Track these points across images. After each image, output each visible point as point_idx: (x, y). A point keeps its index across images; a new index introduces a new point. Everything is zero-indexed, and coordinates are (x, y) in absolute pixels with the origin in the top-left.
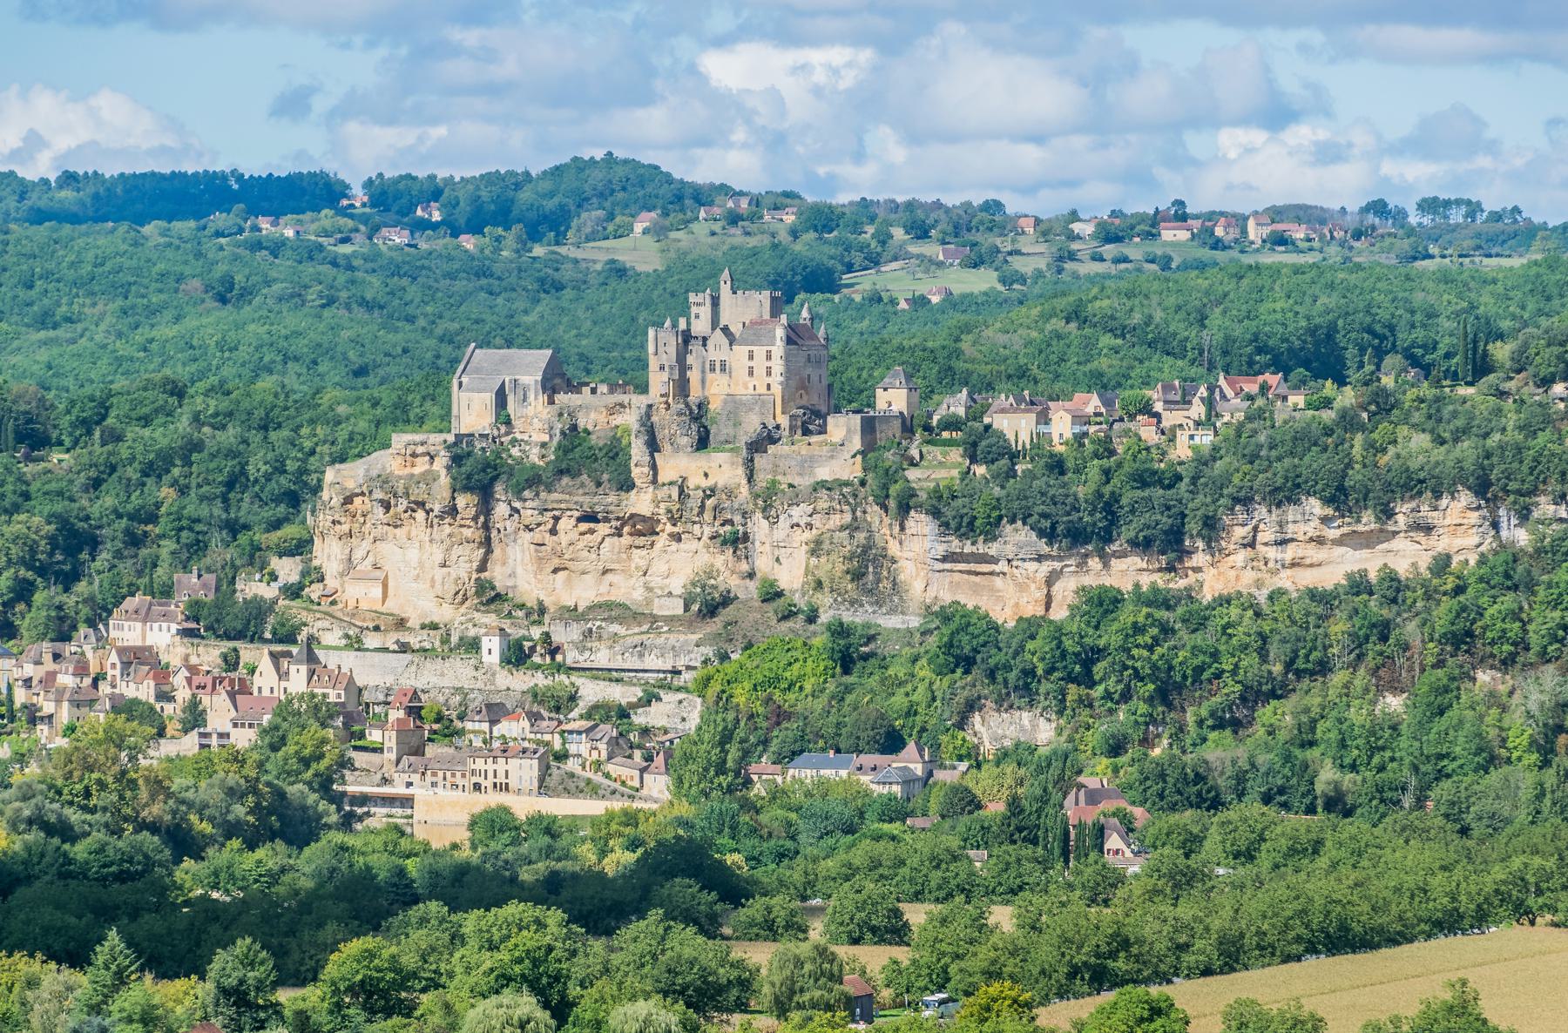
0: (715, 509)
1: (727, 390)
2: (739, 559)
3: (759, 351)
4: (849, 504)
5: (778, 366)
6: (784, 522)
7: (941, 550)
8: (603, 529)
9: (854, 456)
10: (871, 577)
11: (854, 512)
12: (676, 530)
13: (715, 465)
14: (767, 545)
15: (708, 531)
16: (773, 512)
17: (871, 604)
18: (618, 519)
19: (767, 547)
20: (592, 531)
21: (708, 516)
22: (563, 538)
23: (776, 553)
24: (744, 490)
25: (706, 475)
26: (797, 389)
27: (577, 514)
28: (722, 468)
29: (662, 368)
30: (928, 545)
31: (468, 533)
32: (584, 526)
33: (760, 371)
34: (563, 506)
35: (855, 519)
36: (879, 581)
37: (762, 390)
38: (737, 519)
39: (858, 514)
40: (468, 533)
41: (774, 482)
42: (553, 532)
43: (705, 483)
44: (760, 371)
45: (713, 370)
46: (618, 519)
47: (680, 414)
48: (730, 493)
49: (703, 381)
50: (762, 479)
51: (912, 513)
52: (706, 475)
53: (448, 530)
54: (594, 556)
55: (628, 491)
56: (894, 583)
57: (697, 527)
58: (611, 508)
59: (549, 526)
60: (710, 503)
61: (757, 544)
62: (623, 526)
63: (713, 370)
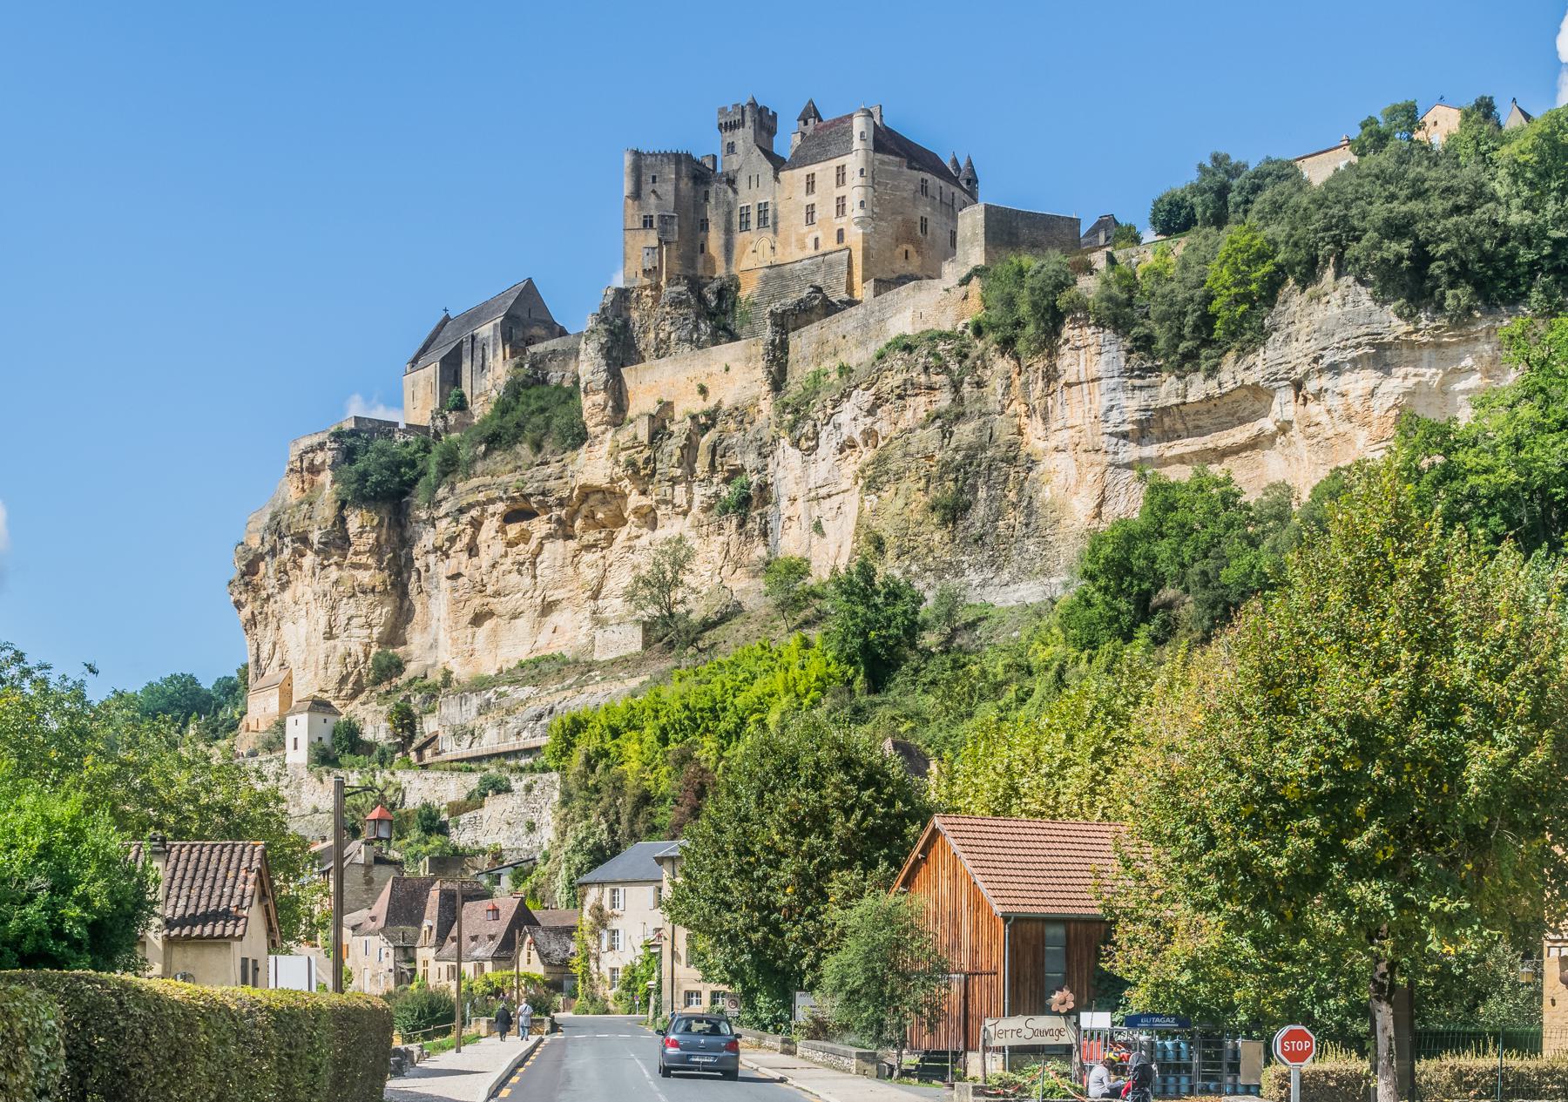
1: (768, 258)
2: (749, 537)
3: (824, 171)
4: (946, 369)
5: (854, 191)
6: (827, 447)
7: (1132, 406)
8: (540, 527)
9: (965, 281)
11: (956, 387)
13: (717, 368)
15: (700, 493)
16: (808, 428)
18: (561, 503)
20: (525, 537)
21: (701, 466)
22: (485, 559)
23: (816, 513)
24: (767, 407)
25: (703, 390)
26: (898, 241)
27: (501, 507)
28: (732, 374)
29: (647, 223)
30: (1102, 403)
31: (364, 577)
32: (513, 530)
33: (825, 210)
34: (481, 497)
35: (958, 399)
36: (999, 515)
37: (829, 244)
38: (751, 460)
39: (966, 389)
40: (364, 577)
41: (816, 376)
42: (472, 550)
43: (699, 405)
45: (745, 226)
46: (561, 503)
47: (677, 303)
48: (741, 414)
50: (799, 374)
51: (1067, 332)
52: (703, 390)
53: (334, 573)
54: (527, 580)
55: (575, 447)
56: (1030, 511)
57: (680, 490)
58: (551, 484)
59: (466, 539)
60: (706, 440)
61: (784, 503)
62: (572, 517)
63: (745, 226)
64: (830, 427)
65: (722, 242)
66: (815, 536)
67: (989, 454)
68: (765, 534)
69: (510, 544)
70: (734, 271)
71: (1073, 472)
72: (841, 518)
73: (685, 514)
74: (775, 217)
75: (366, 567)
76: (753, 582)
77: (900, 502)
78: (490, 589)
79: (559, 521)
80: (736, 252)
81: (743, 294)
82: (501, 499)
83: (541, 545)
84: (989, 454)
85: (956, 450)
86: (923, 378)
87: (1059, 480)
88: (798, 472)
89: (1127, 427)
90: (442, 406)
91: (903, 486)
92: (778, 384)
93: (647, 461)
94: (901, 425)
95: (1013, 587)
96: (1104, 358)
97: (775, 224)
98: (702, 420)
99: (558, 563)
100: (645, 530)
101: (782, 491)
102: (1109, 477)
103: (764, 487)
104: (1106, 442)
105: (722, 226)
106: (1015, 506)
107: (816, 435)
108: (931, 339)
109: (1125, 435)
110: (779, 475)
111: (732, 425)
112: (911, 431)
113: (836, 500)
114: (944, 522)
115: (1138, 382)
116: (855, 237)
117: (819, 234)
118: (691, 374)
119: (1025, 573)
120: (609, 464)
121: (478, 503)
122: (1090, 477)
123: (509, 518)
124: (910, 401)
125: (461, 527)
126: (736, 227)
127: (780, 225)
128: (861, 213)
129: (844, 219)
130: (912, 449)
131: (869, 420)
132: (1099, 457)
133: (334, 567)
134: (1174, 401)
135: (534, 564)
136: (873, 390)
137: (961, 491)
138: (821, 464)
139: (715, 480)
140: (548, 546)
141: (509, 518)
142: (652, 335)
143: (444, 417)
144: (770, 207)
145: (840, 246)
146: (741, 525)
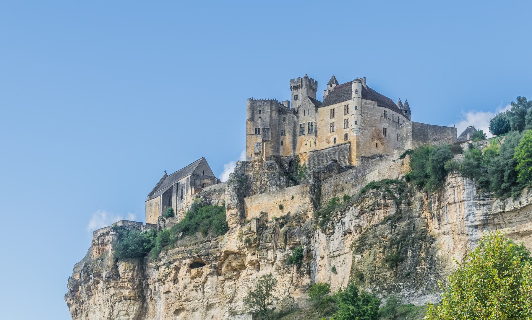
0: (286, 234)
1: (313, 147)
2: (302, 274)
3: (339, 107)
4: (394, 198)
5: (353, 117)
6: (338, 233)
7: (479, 213)
8: (206, 270)
9: (402, 157)
10: (409, 261)
11: (398, 204)
12: (255, 258)
13: (288, 197)
14: (326, 259)
15: (280, 255)
16: (329, 225)
17: (408, 288)
18: (216, 259)
19: (326, 259)
20: (199, 274)
22: (181, 284)
24: (311, 214)
25: (281, 207)
27: (188, 261)
28: (296, 201)
30: (465, 211)
32: (194, 271)
33: (339, 125)
34: (179, 256)
35: (399, 211)
36: (417, 263)
38: (303, 239)
39: (403, 206)
40: (126, 292)
41: (334, 200)
42: (175, 280)
43: (279, 214)
44: (339, 125)
46: (216, 259)
47: (270, 167)
48: (299, 218)
49: (294, 143)
50: (326, 199)
51: (449, 179)
52: (281, 207)
54: (200, 294)
55: (223, 234)
56: (432, 262)
58: (212, 250)
59: (172, 276)
61: (318, 259)
63: (302, 132)
64: (340, 224)
65: (291, 140)
66: (333, 274)
67: (413, 236)
68: (309, 273)
69: (193, 278)
70: (297, 153)
71: (452, 244)
72: (344, 265)
73: (273, 264)
74: (316, 128)
75: (127, 288)
76: (303, 295)
77: (371, 258)
78: (183, 298)
79: (215, 267)
80: (298, 145)
81: (301, 164)
82: (189, 257)
83: (206, 278)
84: (413, 236)
85: (398, 234)
86: (382, 201)
87: (445, 248)
88: (325, 245)
89: (477, 223)
90: (162, 215)
91: (373, 251)
92: (316, 204)
93: (255, 240)
94: (372, 223)
95: (423, 297)
96: (466, 191)
97: (316, 132)
98: (281, 221)
99: (215, 286)
100: (254, 271)
101: (318, 253)
102: (468, 246)
103: (309, 251)
104: (466, 230)
105: (292, 133)
106: (425, 259)
107: (334, 227)
108: (387, 183)
109: (476, 227)
110: (316, 246)
111: (295, 223)
112: (377, 225)
113: (342, 257)
114: (391, 267)
115: (482, 202)
116: (353, 137)
117: (336, 136)
118: (276, 200)
119: (428, 291)
120: (238, 241)
121: (178, 259)
122: (460, 246)
123: (192, 266)
124: (377, 212)
125: (170, 270)
126: (298, 133)
127: (318, 132)
128: (354, 126)
129: (348, 130)
130: (377, 234)
131: (357, 221)
132: (464, 237)
133: (112, 288)
134: (499, 211)
135: (203, 286)
136: (359, 207)
137: (399, 253)
138: (335, 241)
139: (287, 248)
140: (210, 278)
141: (192, 266)
142: (259, 183)
143: (164, 220)
144: (314, 124)
145: (346, 142)
146: (298, 269)
